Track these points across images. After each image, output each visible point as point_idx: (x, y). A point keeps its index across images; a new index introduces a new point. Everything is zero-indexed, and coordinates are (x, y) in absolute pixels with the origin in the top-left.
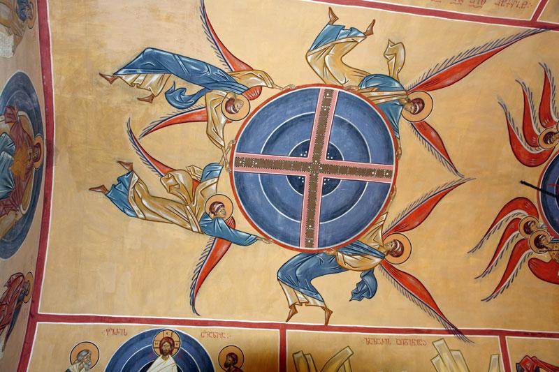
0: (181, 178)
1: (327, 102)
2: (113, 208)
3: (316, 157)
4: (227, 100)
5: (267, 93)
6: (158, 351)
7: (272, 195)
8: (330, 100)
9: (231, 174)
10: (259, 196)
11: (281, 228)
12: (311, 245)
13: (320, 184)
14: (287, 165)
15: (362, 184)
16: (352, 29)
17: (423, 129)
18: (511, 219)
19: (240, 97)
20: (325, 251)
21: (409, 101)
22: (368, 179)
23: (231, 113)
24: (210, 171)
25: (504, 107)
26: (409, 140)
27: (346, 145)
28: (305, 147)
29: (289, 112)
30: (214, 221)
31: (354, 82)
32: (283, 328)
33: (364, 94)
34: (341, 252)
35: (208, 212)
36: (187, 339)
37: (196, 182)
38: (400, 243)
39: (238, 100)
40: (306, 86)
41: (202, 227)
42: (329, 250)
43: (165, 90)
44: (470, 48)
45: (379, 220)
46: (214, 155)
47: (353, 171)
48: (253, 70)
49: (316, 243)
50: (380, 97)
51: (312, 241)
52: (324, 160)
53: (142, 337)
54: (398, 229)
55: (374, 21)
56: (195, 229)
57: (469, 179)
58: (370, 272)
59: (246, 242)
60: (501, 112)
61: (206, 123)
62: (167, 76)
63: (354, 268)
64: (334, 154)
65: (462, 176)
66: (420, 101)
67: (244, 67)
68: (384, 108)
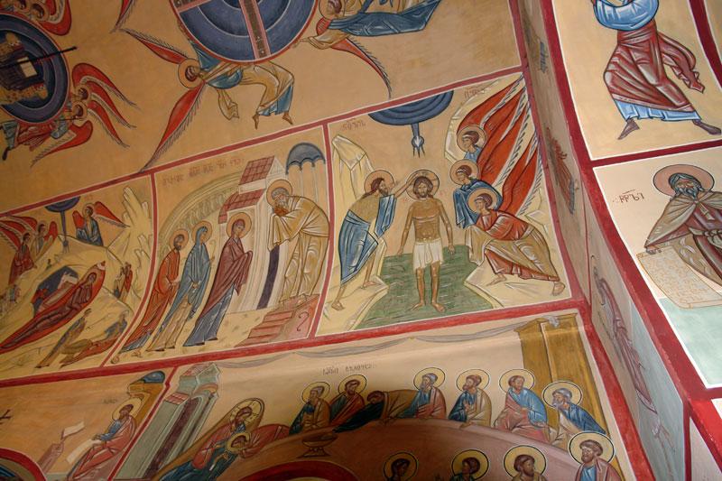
1: (260, 45)
5: (311, 31)
8: (258, 47)
16: (269, 114)
17: (176, 57)
18: (58, 12)
19: (333, 17)
21: (199, 76)
25: (131, 103)
26: (178, 40)
29: (286, 22)
31: (248, 72)
39: (332, 14)
40: (282, 52)
48: (331, 47)
50: (222, 68)
55: (256, 128)
57: (114, 30)
60: (129, 98)
62: (401, 10)
66: (192, 79)
67: (339, 46)
68: (215, 61)
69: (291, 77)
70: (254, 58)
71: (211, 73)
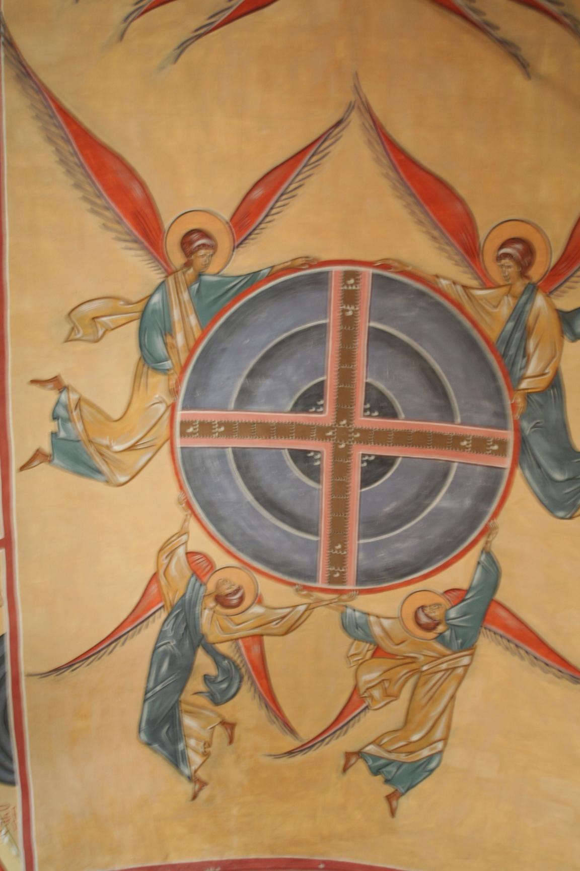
0: (369, 677)
1: (206, 429)
2: (426, 786)
3: (321, 432)
4: (219, 608)
5: (199, 540)
7: (399, 518)
8: (202, 424)
9: (362, 592)
10: (402, 542)
11: (468, 502)
12: (503, 444)
13: (376, 422)
14: (340, 489)
15: (376, 336)
16: (55, 417)
17: (247, 219)
20: (517, 416)
21: (188, 265)
22: (364, 324)
23: (242, 599)
24: (356, 629)
25: (183, 47)
26: (278, 243)
27: (293, 377)
28: (302, 458)
30: (451, 627)
33: (183, 361)
34: (522, 378)
35: (432, 635)
37: (378, 652)
38: (503, 246)
39: (217, 587)
40: (177, 474)
41: (463, 647)
42: (514, 406)
43: (210, 706)
44: (60, 170)
45: (453, 295)
46: (325, 619)
47: (347, 356)
48: (155, 575)
49: (499, 433)
50: (186, 323)
51: (495, 442)
52: (326, 415)
54: (470, 251)
55: (34, 382)
56: (466, 661)
57: (357, 89)
58: (566, 319)
59: (491, 572)
60: (196, 51)
61: (266, 639)
62: (184, 706)
63: (556, 354)
64: (310, 399)
65: (350, 108)
66: (186, 242)
67: (154, 589)
69: (123, 479)
70: (184, 408)
71: (185, 296)
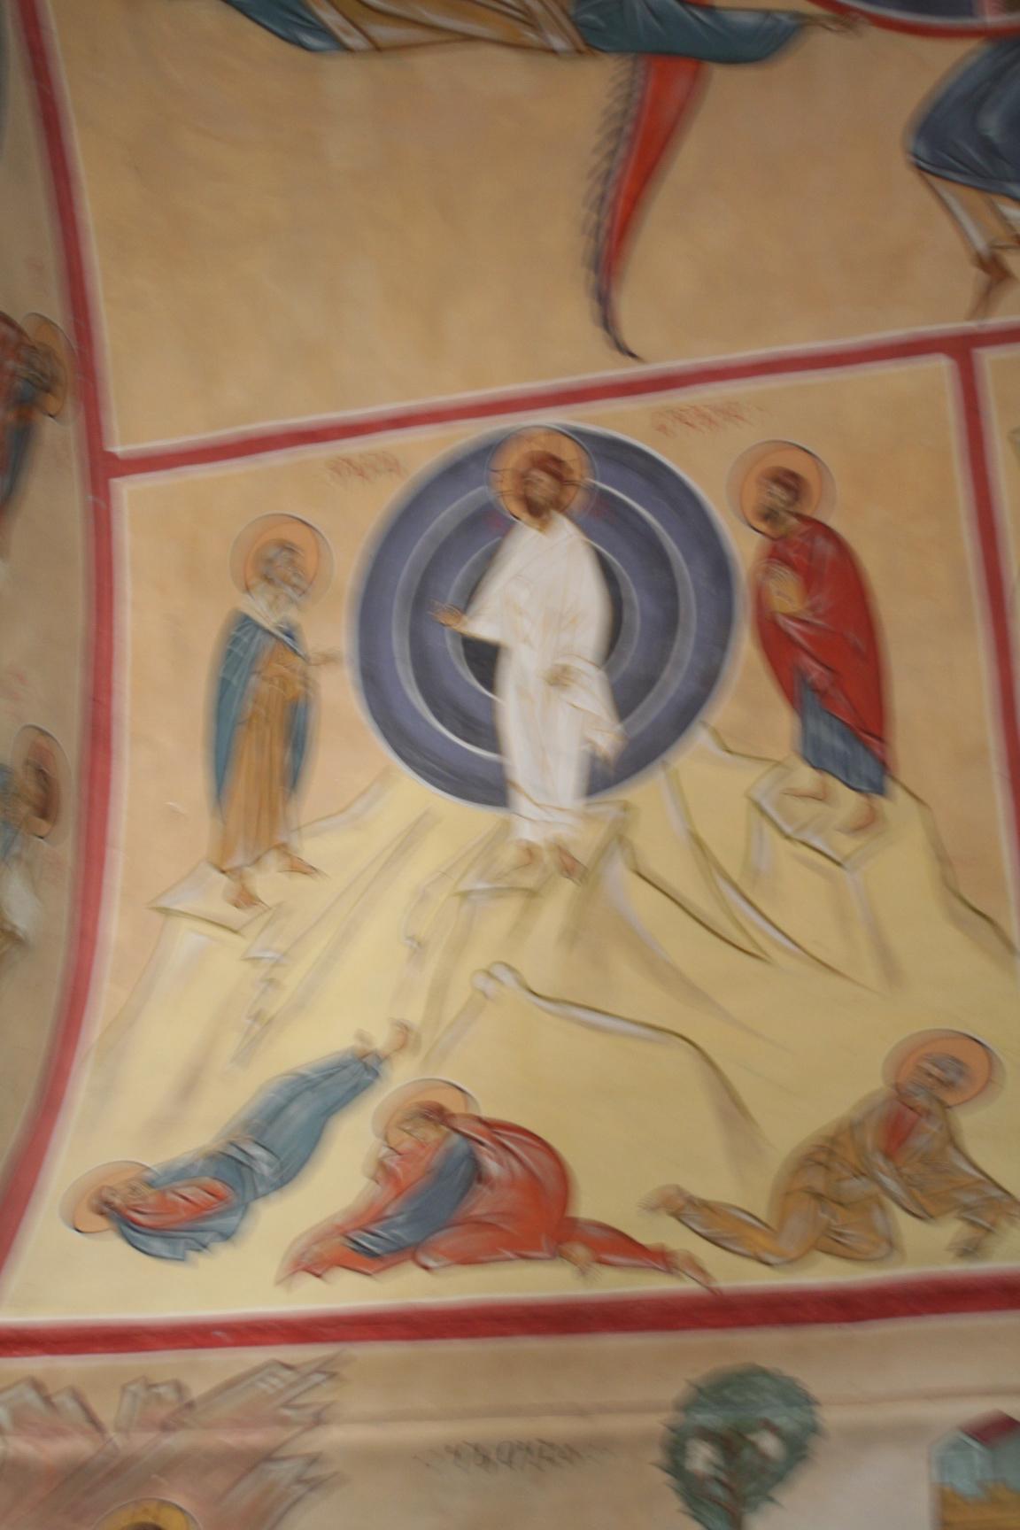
2: (259, 40)
6: (514, 507)
32: (961, 348)
36: (613, 453)
53: (456, 471)
56: (558, 43)
